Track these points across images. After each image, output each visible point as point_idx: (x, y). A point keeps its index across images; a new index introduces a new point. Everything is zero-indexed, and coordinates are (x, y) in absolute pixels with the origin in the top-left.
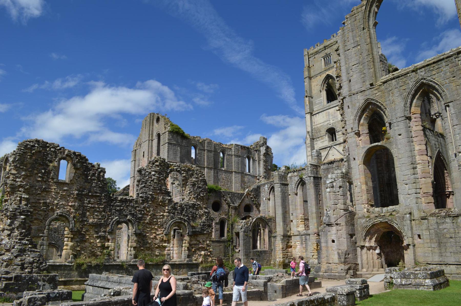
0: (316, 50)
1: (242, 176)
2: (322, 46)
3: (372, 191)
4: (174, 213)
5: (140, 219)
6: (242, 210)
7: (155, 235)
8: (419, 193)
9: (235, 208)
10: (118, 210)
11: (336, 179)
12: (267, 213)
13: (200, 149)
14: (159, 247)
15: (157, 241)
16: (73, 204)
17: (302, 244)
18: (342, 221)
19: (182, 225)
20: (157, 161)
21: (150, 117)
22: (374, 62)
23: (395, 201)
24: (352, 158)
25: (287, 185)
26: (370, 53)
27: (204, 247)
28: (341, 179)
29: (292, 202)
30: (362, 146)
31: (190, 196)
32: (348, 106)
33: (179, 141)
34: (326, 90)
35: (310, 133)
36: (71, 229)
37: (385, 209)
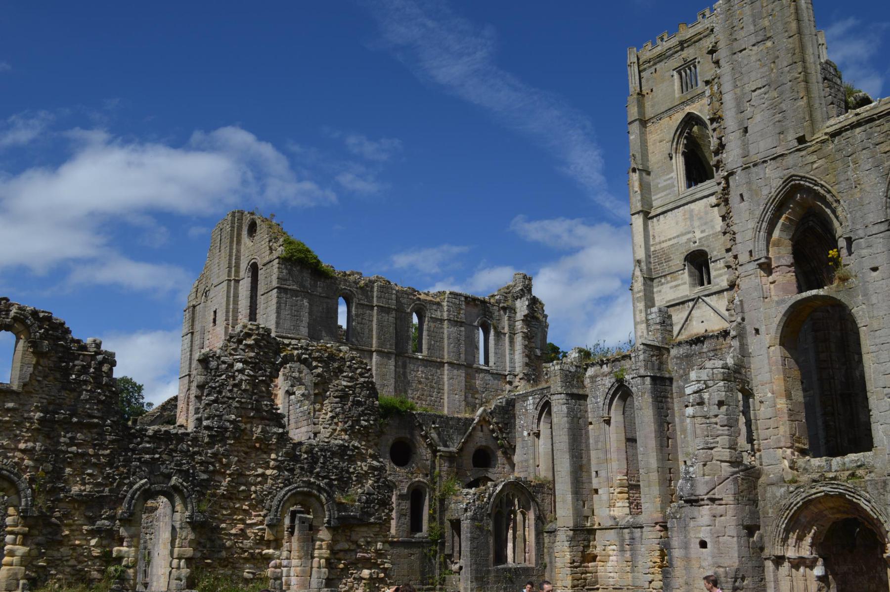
0: (658, 50)
1: (467, 374)
2: (674, 41)
3: (804, 414)
4: (291, 471)
5: (205, 484)
6: (468, 460)
7: (241, 526)
9: (450, 458)
10: (146, 463)
11: (710, 383)
12: (531, 469)
13: (360, 305)
14: (252, 558)
15: (248, 543)
16: (30, 445)
17: (622, 550)
18: (726, 492)
19: (313, 500)
20: (248, 335)
21: (233, 222)
22: (806, 81)
23: (862, 440)
24: (750, 330)
25: (584, 397)
26: (797, 58)
27: (370, 559)
28: (722, 383)
29: (597, 442)
30: (776, 298)
31: (333, 427)
32: (741, 195)
33: (307, 284)
34: (684, 154)
35: (643, 264)
36: (24, 511)
37: (836, 461)
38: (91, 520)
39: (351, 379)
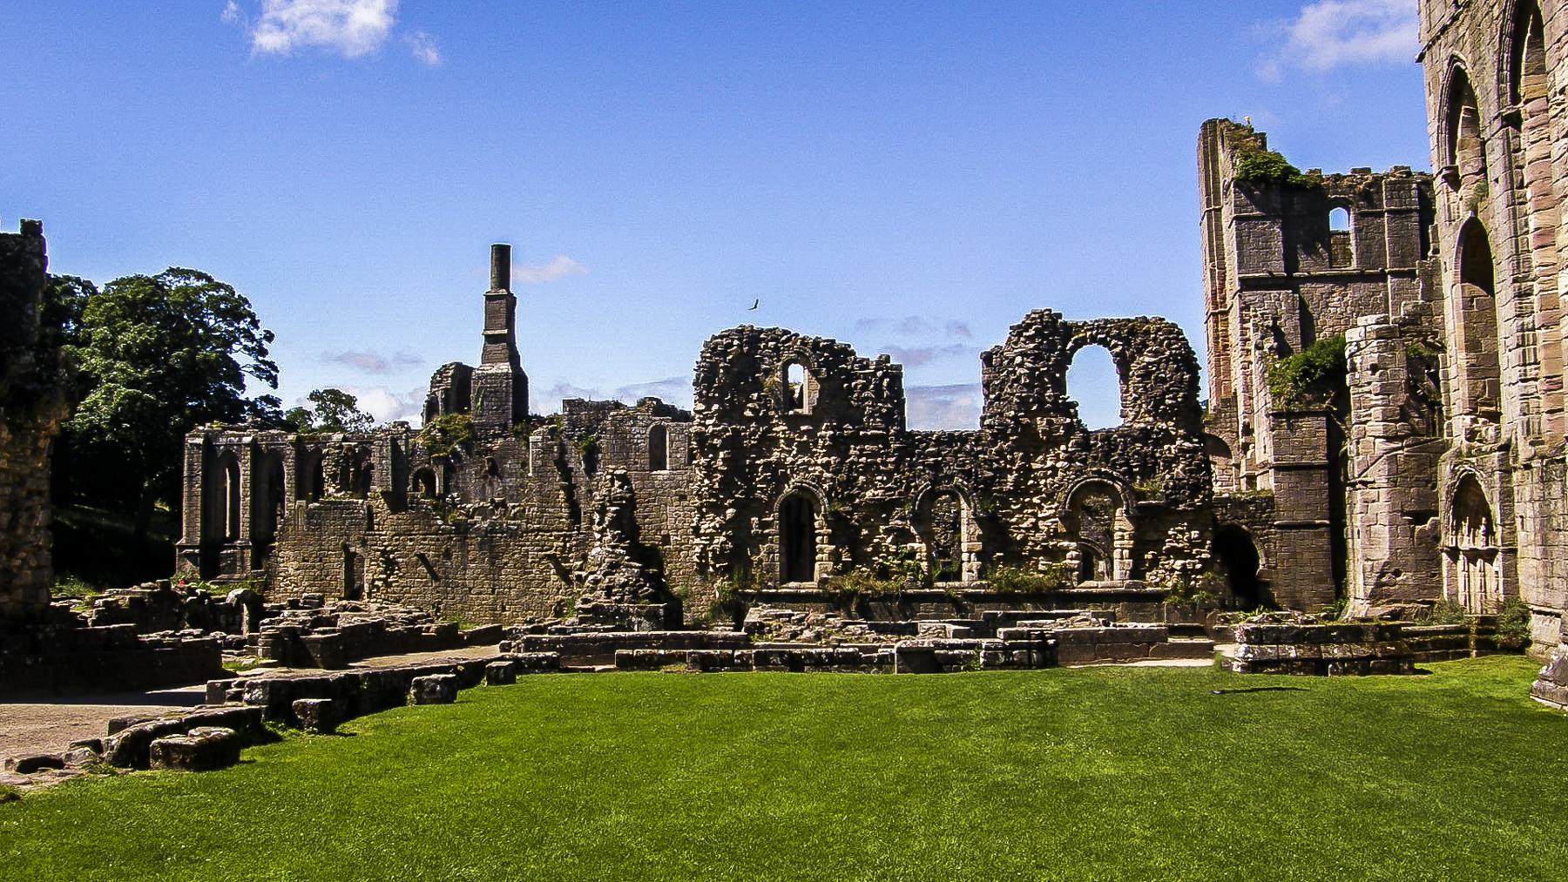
4: (1084, 461)
5: (989, 482)
8: (1535, 379)
10: (930, 466)
16: (826, 459)
38: (886, 521)
39: (1156, 353)
